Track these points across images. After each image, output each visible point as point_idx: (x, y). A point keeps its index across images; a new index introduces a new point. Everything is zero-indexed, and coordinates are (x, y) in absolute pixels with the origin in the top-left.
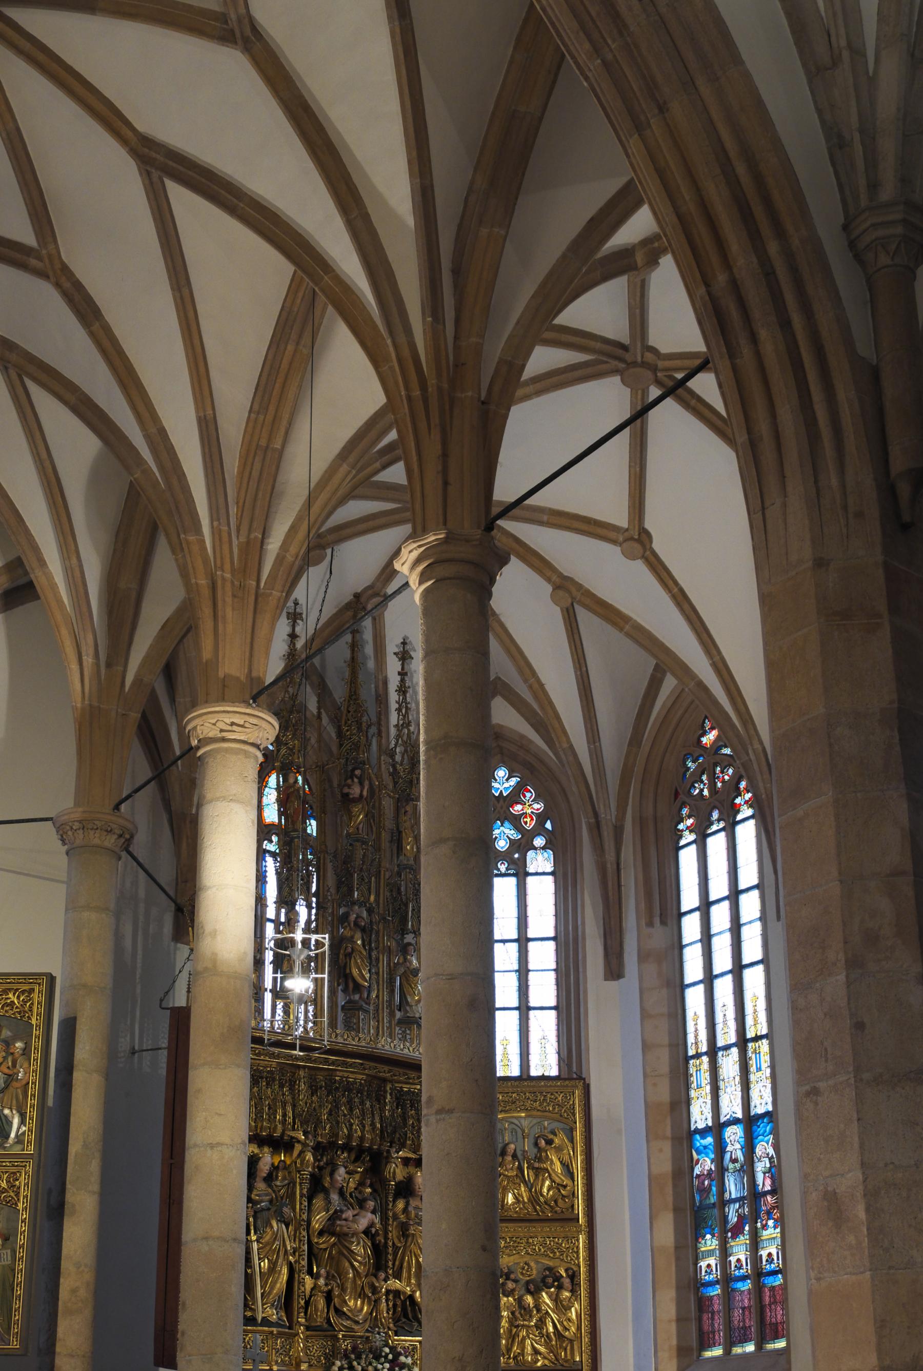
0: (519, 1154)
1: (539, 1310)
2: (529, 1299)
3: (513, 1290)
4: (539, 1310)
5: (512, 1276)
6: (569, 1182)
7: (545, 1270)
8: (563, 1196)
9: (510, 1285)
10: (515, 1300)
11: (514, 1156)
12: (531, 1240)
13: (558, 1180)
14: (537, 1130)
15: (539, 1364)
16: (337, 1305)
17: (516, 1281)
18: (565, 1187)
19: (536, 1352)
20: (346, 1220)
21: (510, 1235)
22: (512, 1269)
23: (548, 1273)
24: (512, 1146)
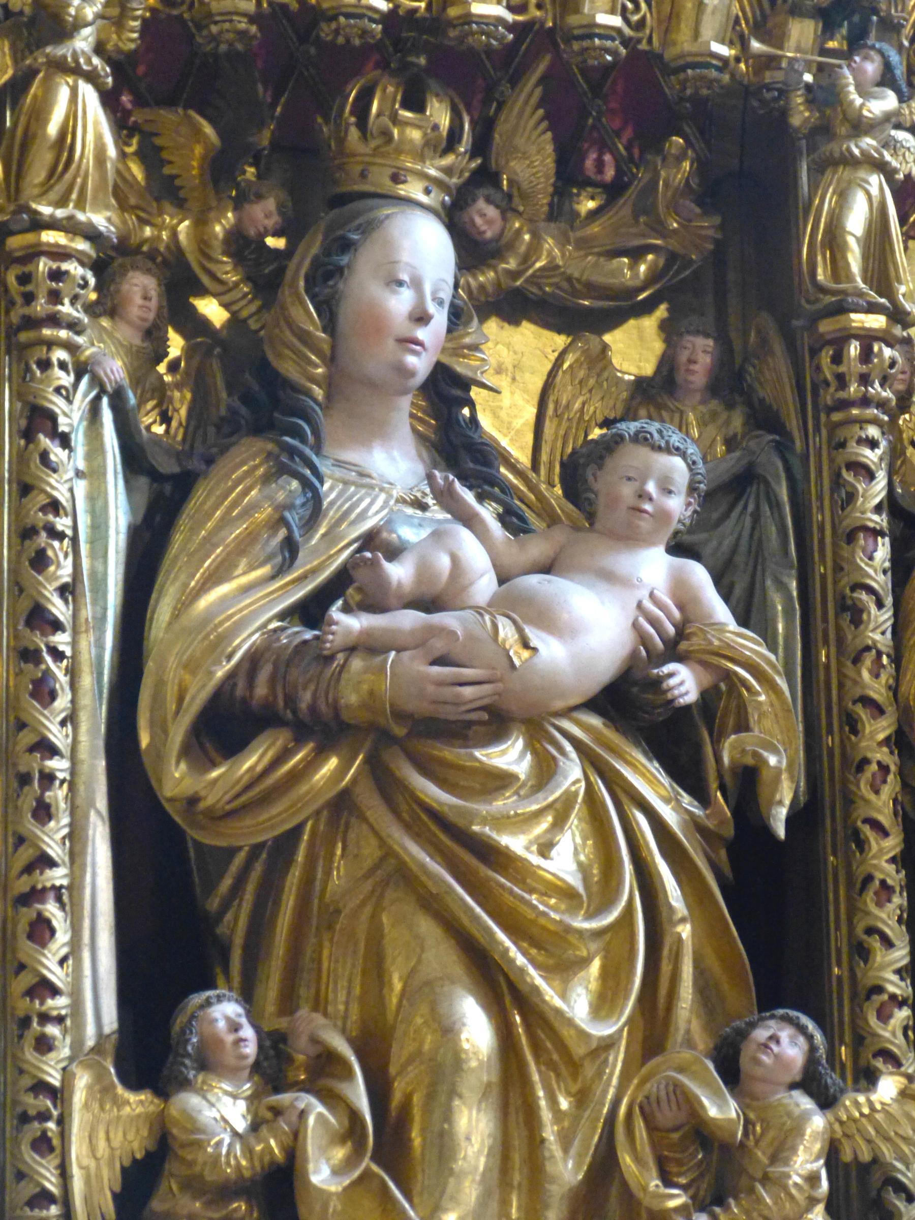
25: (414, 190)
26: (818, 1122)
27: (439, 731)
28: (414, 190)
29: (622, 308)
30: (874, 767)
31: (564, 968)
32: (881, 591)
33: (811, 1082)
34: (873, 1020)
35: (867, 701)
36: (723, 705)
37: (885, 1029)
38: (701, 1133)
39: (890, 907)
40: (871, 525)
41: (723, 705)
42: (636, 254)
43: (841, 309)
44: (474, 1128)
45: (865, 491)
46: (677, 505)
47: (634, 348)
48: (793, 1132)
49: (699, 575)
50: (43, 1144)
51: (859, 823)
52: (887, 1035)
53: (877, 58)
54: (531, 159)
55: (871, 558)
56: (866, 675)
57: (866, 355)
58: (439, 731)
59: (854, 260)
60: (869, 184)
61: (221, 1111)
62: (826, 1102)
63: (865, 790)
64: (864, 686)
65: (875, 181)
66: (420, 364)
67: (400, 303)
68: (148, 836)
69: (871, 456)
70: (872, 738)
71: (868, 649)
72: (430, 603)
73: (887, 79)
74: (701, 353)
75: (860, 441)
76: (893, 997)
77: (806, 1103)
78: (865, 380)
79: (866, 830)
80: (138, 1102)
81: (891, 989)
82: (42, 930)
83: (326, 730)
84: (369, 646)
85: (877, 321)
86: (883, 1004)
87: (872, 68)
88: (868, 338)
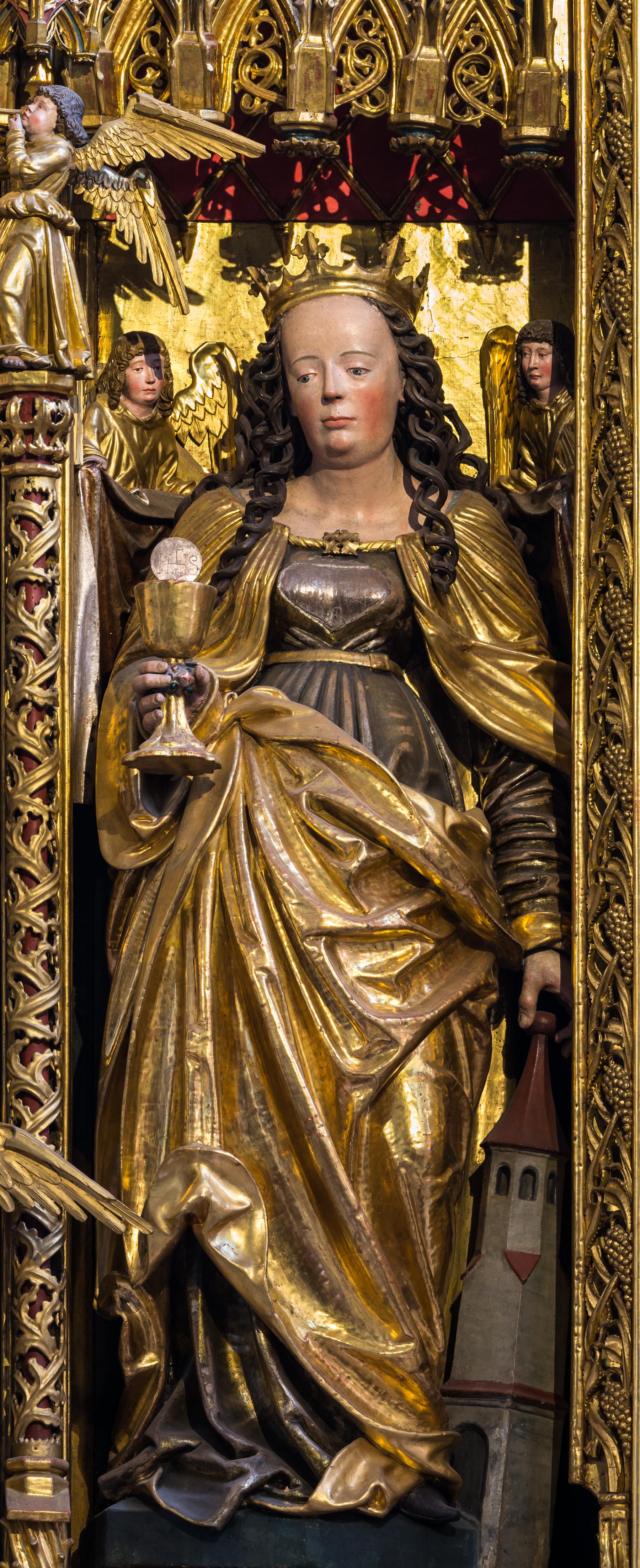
30: (26, 818)
32: (41, 644)
34: (16, 1063)
35: (22, 753)
37: (25, 1072)
39: (35, 954)
40: (33, 578)
45: (29, 545)
51: (12, 873)
52: (27, 1078)
53: (51, 105)
55: (33, 613)
56: (22, 729)
57: (28, 410)
60: (34, 241)
63: (16, 842)
64: (20, 740)
65: (40, 235)
69: (37, 509)
70: (24, 790)
71: (25, 702)
73: (62, 128)
75: (27, 495)
76: (34, 1040)
78: (29, 434)
79: (17, 880)
81: (32, 1033)
85: (43, 377)
86: (25, 1048)
88: (31, 393)
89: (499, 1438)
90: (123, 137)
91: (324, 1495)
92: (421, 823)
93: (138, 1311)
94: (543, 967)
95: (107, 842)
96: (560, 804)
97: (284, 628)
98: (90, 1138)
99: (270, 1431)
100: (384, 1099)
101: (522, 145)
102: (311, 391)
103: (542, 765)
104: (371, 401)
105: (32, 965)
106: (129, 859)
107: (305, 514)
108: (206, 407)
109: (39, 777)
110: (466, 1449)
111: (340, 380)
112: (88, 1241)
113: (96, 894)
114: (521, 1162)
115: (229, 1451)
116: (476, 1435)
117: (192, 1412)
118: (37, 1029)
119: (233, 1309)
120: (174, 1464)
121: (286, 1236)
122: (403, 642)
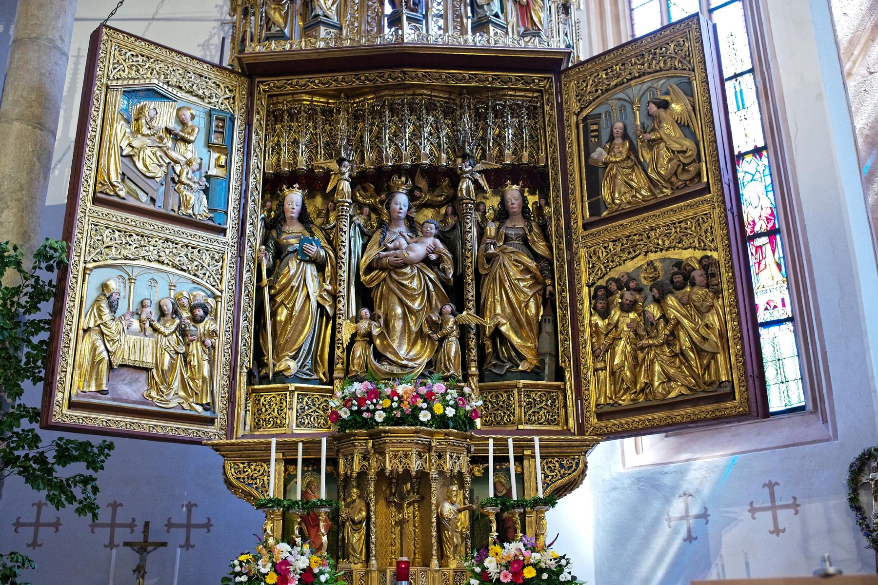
0: (631, 133)
1: (667, 322)
2: (654, 311)
3: (635, 302)
4: (667, 322)
5: (632, 285)
6: (688, 143)
7: (674, 266)
8: (685, 165)
9: (628, 296)
10: (639, 315)
11: (625, 136)
12: (652, 234)
13: (676, 147)
14: (648, 97)
15: (672, 395)
16: (380, 349)
17: (639, 290)
18: (684, 152)
19: (669, 379)
20: (396, 249)
21: (627, 233)
22: (634, 276)
23: (676, 269)
24: (619, 125)
25: (401, 190)
26: (452, 319)
27: (397, 267)
28: (401, 190)
29: (440, 205)
31: (413, 300)
33: (453, 314)
36: (440, 260)
38: (434, 322)
41: (440, 260)
42: (441, 196)
43: (462, 200)
44: (398, 325)
46: (434, 231)
47: (443, 211)
48: (448, 321)
49: (438, 241)
50: (339, 332)
54: (423, 184)
58: (397, 267)
59: (464, 193)
61: (364, 325)
62: (455, 316)
66: (402, 216)
67: (398, 206)
68: (359, 286)
72: (396, 249)
73: (470, 165)
74: (450, 209)
77: (451, 316)
80: (354, 325)
82: (340, 302)
83: (383, 269)
84: (386, 256)
87: (468, 164)
88: (467, 203)
89: (547, 360)
90: (479, 167)
91: (520, 368)
92: (532, 264)
93: (488, 343)
94: (550, 288)
95: (480, 271)
96: (551, 264)
97: (507, 239)
98: (480, 311)
99: (510, 359)
100: (527, 306)
101: (540, 167)
102: (510, 204)
103: (547, 260)
104: (519, 205)
105: (470, 288)
106: (484, 272)
107: (508, 224)
108: (490, 214)
109: (470, 260)
110: (542, 362)
111: (514, 201)
112: (480, 328)
113: (478, 278)
114: (548, 318)
115: (504, 362)
116: (543, 360)
117: (498, 358)
118: (471, 298)
119: (504, 339)
120: (495, 365)
121: (512, 327)
122: (525, 241)
